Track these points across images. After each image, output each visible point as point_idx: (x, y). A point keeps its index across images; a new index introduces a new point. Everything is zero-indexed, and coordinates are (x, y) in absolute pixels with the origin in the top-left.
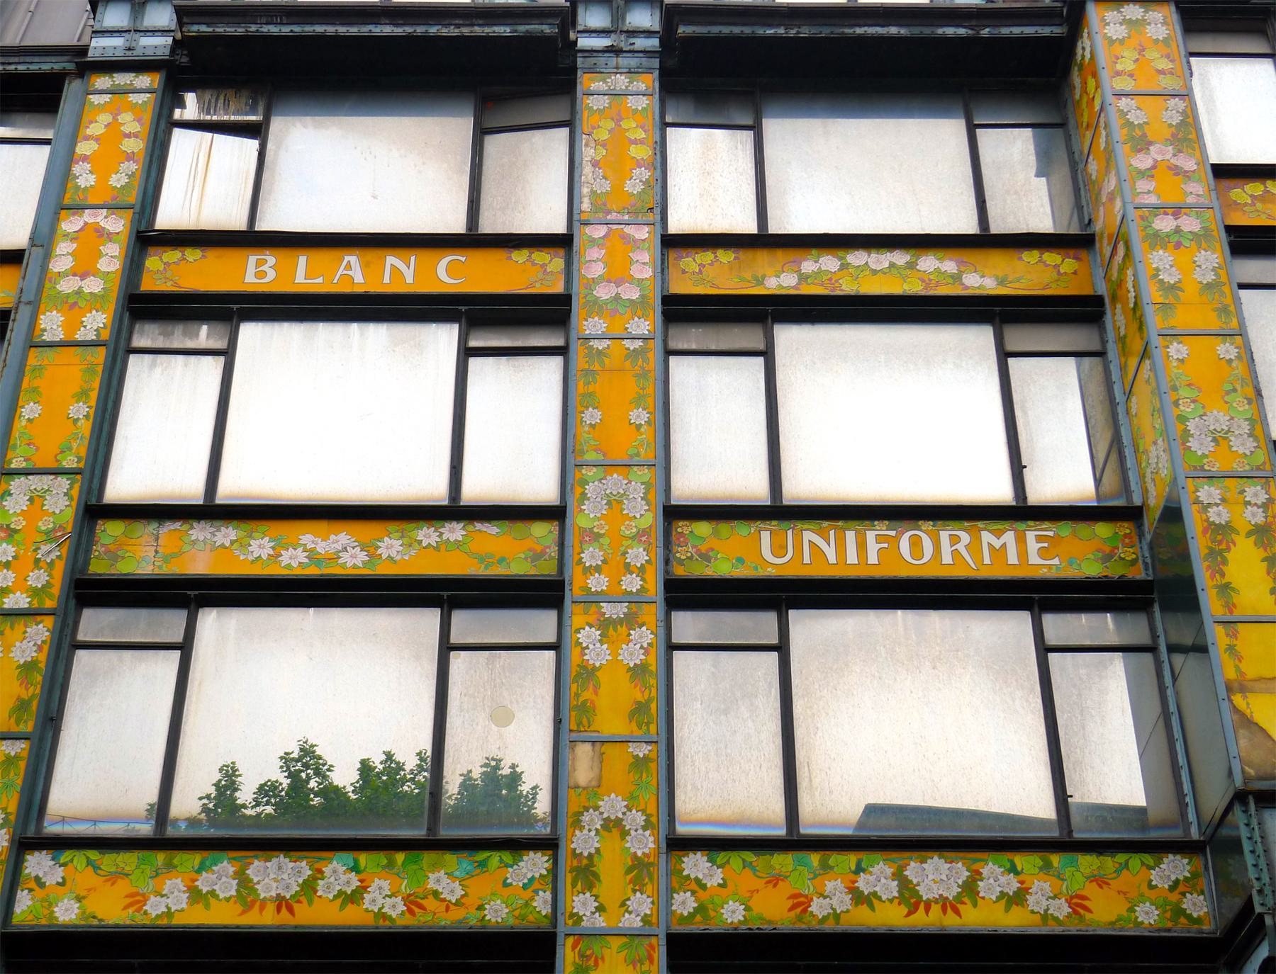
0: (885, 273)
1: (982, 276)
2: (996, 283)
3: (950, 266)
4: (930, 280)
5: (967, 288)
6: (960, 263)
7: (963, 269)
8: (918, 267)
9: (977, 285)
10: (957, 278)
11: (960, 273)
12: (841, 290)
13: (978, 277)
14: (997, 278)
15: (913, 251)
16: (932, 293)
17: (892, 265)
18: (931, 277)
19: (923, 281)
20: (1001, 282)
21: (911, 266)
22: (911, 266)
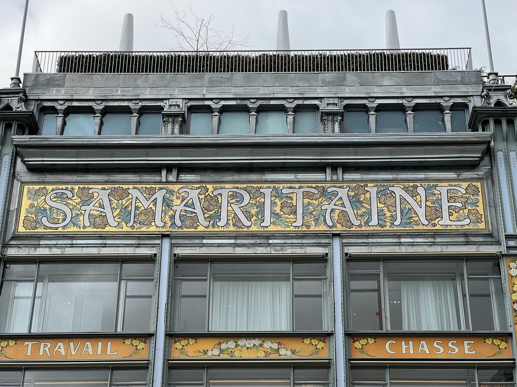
0: (251, 349)
1: (287, 350)
2: (291, 353)
3: (275, 346)
4: (268, 352)
5: (280, 355)
6: (279, 344)
7: (280, 346)
8: (264, 346)
10: (277, 351)
11: (278, 349)
12: (235, 357)
13: (285, 350)
14: (292, 350)
15: (263, 339)
17: (254, 345)
18: (268, 350)
19: (265, 352)
20: (293, 352)
21: (261, 345)
22: (261, 345)
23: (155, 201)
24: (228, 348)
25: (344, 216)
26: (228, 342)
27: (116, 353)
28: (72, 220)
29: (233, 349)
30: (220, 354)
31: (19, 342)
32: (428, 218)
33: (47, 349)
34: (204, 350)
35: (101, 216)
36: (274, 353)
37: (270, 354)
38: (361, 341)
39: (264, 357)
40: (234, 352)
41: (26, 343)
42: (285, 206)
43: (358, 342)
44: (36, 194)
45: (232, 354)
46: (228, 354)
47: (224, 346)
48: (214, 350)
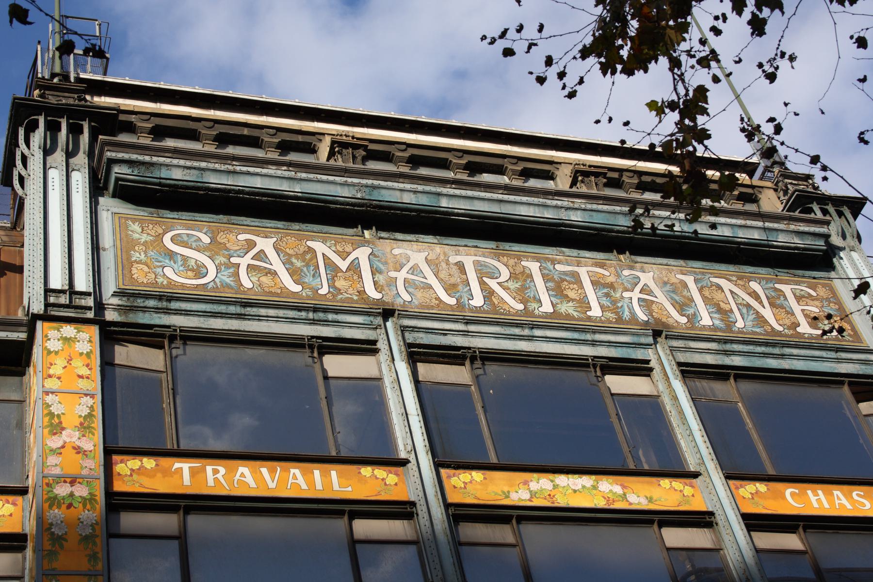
3: (618, 489)
4: (609, 498)
5: (631, 504)
6: (623, 487)
7: (626, 491)
9: (637, 502)
11: (625, 494)
16: (612, 507)
17: (584, 487)
18: (609, 496)
19: (604, 498)
20: (650, 500)
21: (595, 487)
23: (357, 261)
24: (542, 490)
25: (659, 308)
26: (538, 480)
27: (350, 489)
28: (219, 275)
29: (551, 491)
30: (531, 497)
31: (165, 462)
32: (781, 322)
33: (219, 476)
34: (504, 492)
35: (269, 275)
36: (619, 501)
37: (614, 502)
38: (747, 487)
39: (605, 505)
40: (554, 496)
41: (177, 465)
42: (567, 287)
43: (743, 489)
44: (144, 232)
45: (552, 498)
46: (545, 499)
47: (534, 486)
48: (520, 492)
